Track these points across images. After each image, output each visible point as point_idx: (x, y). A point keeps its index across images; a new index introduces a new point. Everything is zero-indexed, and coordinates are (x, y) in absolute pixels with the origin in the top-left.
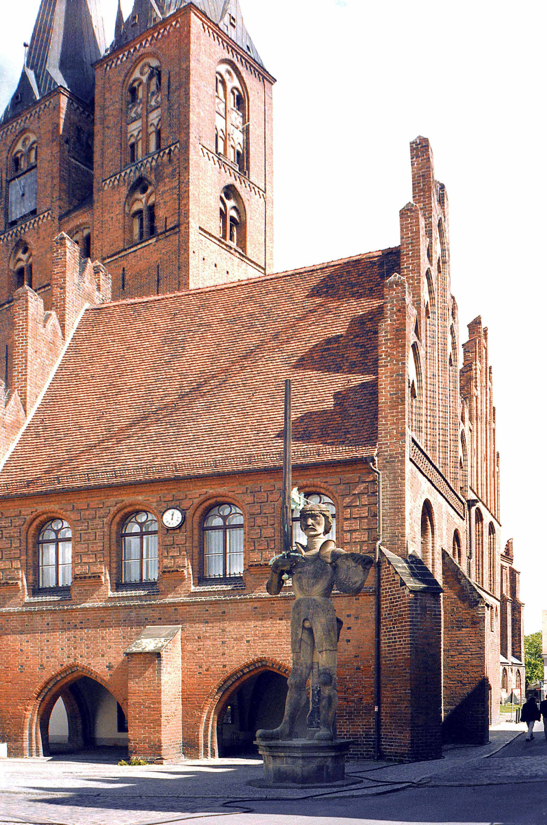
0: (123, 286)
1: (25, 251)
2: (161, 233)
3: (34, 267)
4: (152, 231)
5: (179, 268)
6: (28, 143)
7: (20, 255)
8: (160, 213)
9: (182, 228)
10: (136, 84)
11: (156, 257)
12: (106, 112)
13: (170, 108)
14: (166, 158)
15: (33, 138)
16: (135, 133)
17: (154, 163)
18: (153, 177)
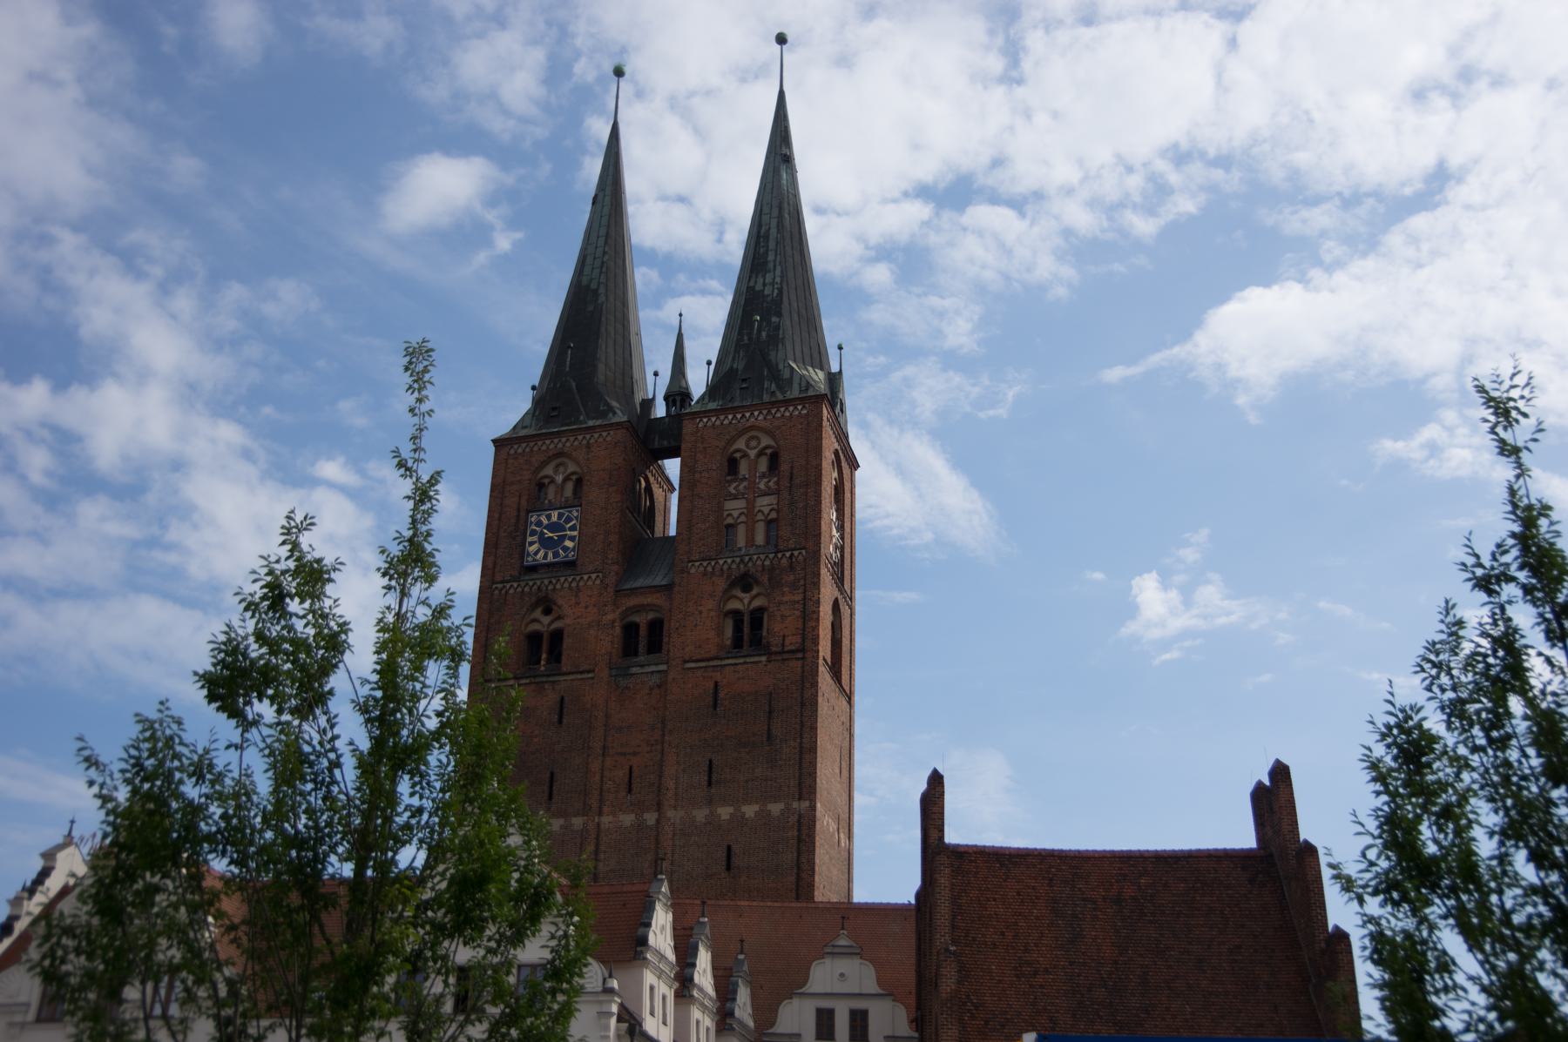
0: (715, 706)
1: (547, 612)
2: (776, 653)
3: (567, 642)
4: (758, 644)
5: (803, 704)
7: (538, 614)
9: (809, 655)
10: (738, 455)
12: (697, 476)
14: (784, 561)
15: (572, 468)
16: (735, 514)
17: (767, 563)
18: (765, 579)
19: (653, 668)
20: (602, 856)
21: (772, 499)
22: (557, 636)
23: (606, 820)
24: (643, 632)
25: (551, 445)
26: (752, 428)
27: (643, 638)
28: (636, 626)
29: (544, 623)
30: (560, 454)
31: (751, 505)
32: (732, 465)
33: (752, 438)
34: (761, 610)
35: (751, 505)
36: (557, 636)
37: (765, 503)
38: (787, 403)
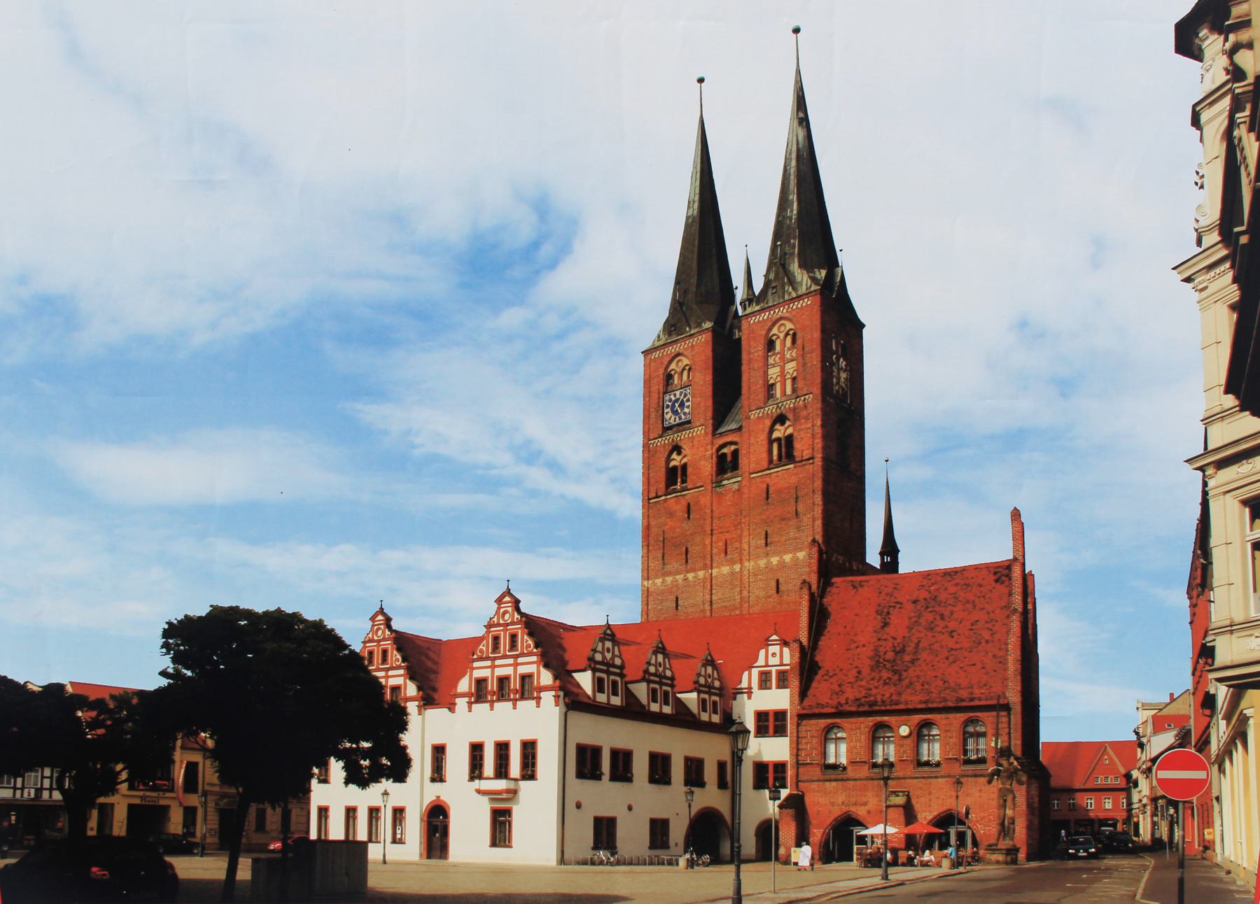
1: (679, 453)
3: (689, 470)
6: (681, 365)
8: (797, 445)
11: (794, 480)
13: (804, 365)
21: (793, 364)
22: (684, 467)
23: (715, 571)
24: (729, 459)
25: (672, 350)
26: (781, 318)
27: (726, 464)
28: (725, 454)
29: (676, 460)
30: (678, 354)
31: (783, 369)
32: (770, 345)
34: (791, 436)
35: (783, 369)
37: (791, 367)
38: (799, 298)
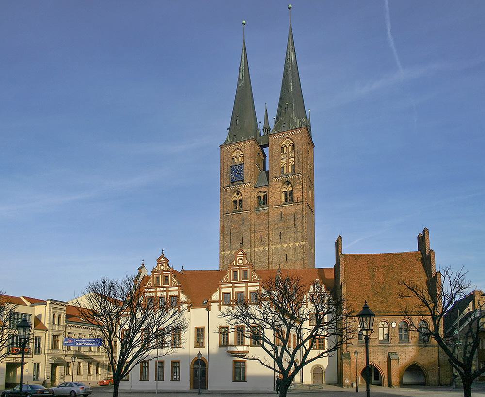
4: (292, 200)
8: (295, 195)
19: (265, 208)
20: (255, 258)
22: (241, 201)
27: (263, 201)
29: (238, 198)
33: (288, 141)
36: (241, 201)
